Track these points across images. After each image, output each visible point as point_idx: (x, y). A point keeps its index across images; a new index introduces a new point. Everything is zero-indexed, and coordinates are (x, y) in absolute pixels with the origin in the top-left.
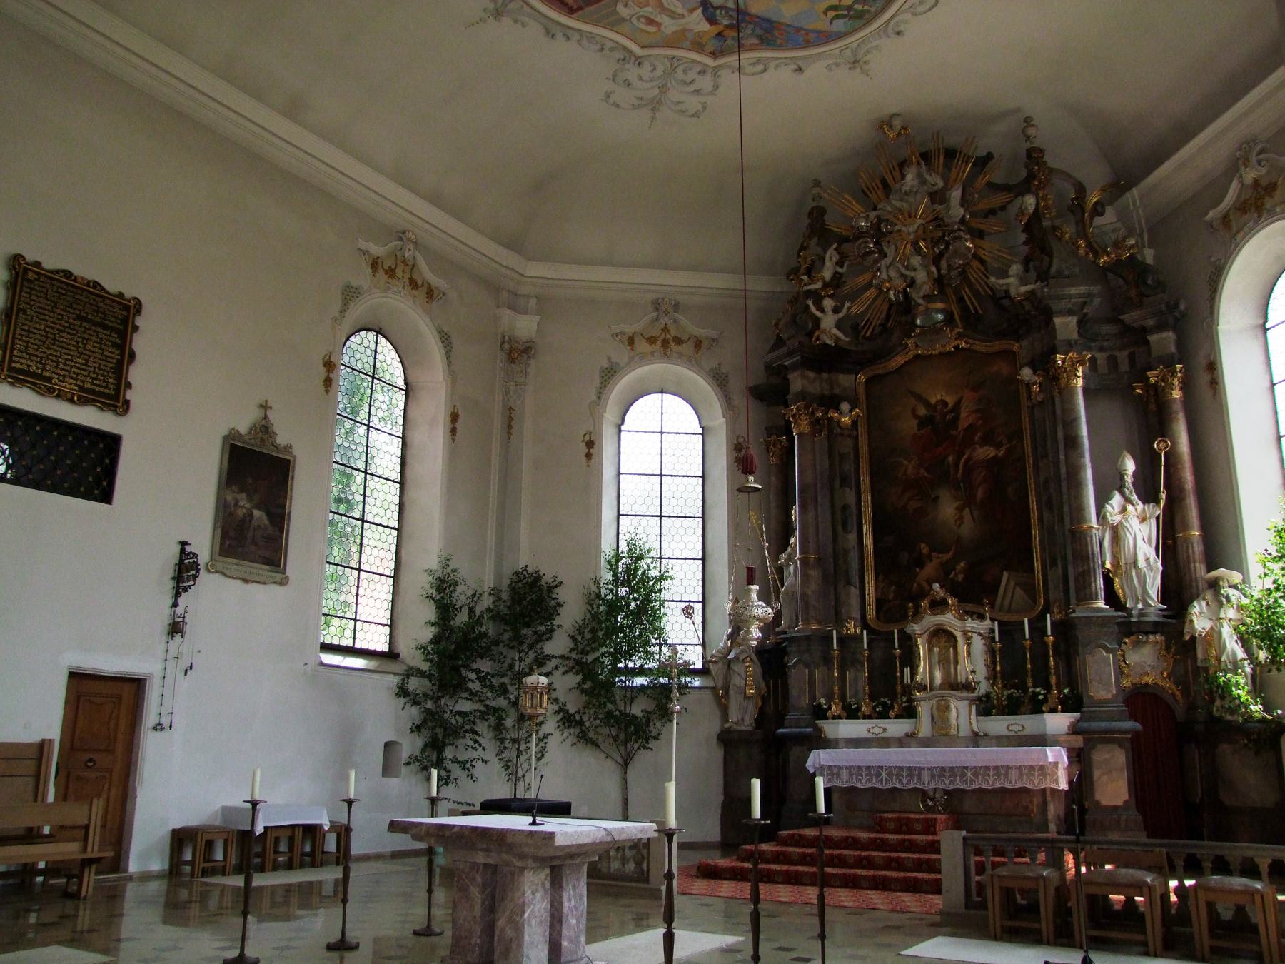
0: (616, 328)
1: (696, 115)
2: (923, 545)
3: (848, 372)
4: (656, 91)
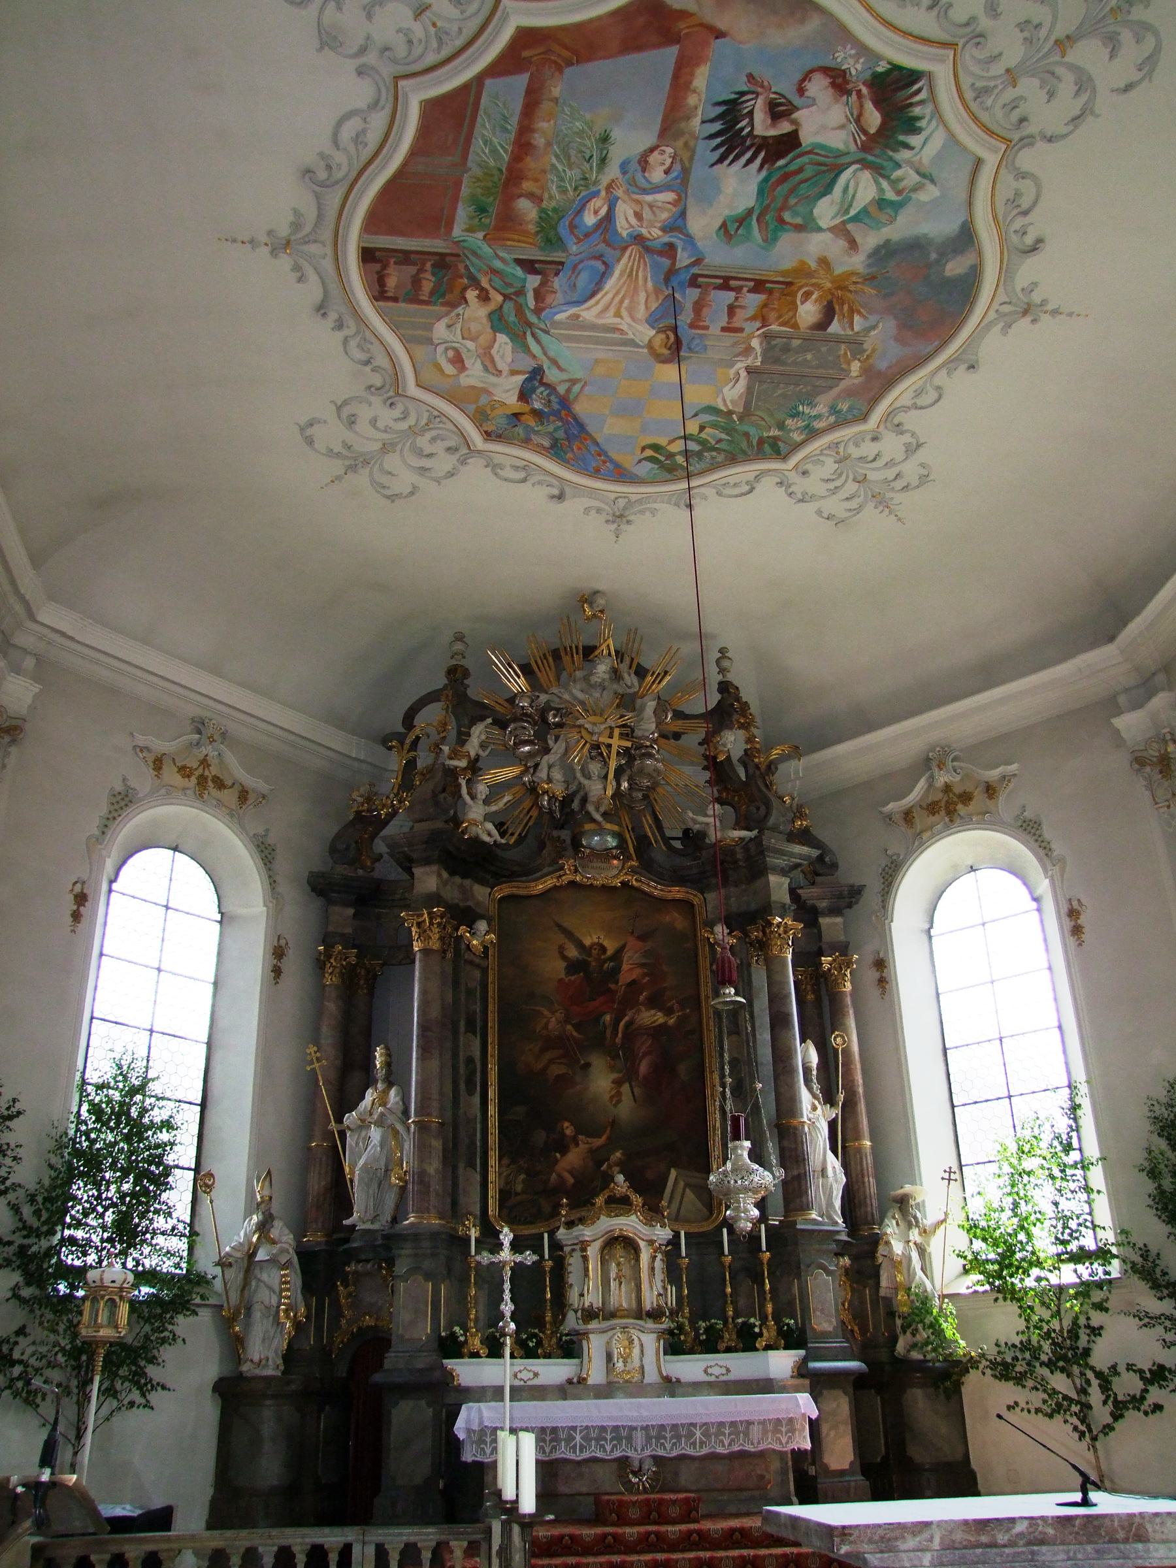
0: (141, 740)
1: (392, 498)
2: (566, 1124)
3: (483, 882)
4: (377, 446)
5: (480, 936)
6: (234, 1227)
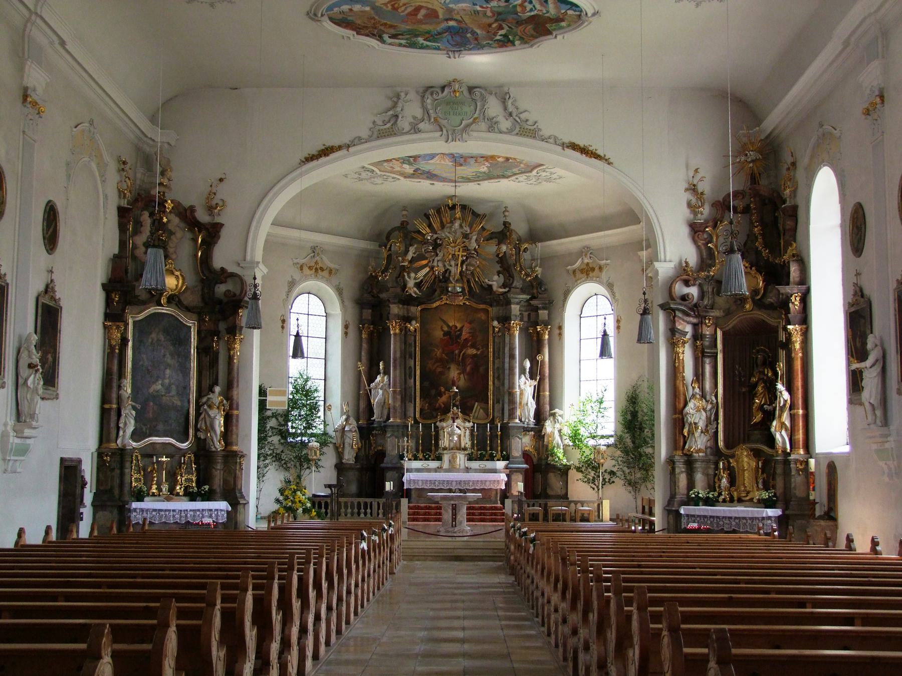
0: (296, 261)
5: (414, 326)
6: (337, 419)
